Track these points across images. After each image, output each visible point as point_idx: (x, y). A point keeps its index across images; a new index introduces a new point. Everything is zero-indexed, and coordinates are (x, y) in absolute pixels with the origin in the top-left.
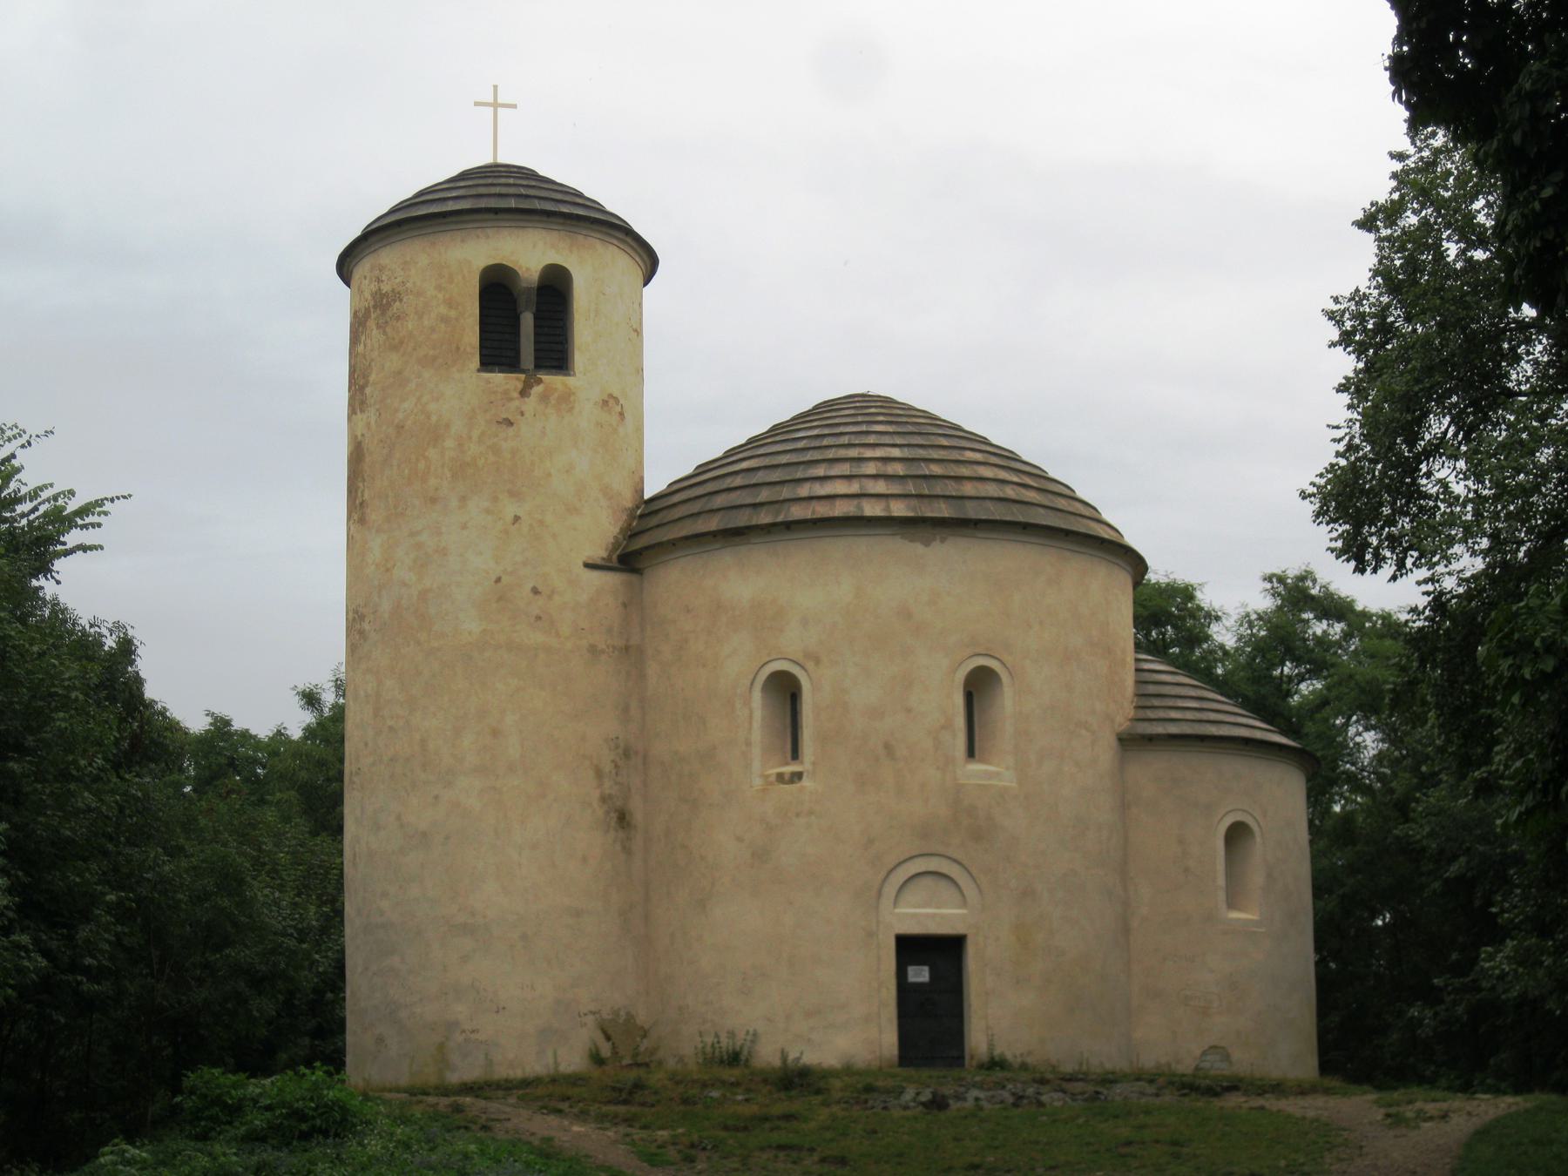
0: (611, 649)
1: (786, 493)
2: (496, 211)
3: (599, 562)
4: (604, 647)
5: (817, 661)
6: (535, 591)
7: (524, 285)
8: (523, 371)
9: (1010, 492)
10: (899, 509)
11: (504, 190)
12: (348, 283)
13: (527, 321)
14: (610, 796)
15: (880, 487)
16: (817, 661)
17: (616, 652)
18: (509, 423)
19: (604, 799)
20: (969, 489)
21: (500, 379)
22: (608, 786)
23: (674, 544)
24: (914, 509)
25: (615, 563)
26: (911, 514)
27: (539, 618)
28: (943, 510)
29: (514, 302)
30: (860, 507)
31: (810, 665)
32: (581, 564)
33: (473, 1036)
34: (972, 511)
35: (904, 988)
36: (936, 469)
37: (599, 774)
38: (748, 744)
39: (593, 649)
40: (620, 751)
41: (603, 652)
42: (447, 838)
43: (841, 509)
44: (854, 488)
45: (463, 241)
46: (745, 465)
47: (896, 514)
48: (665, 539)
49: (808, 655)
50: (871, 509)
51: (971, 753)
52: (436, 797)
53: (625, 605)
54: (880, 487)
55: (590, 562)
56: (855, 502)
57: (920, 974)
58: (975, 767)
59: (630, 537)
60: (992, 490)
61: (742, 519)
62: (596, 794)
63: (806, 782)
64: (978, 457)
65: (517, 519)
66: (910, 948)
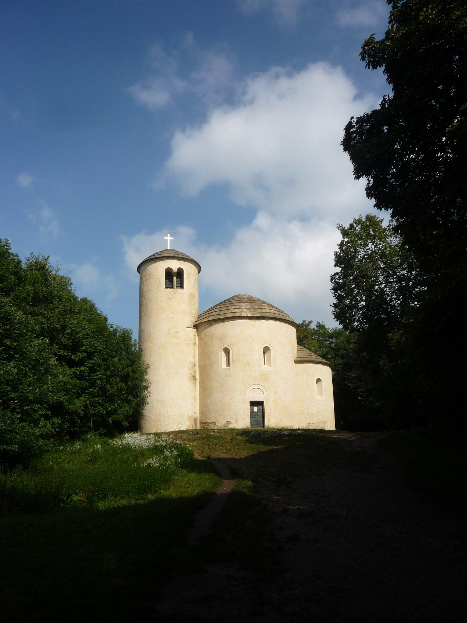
1: (226, 312)
2: (168, 257)
3: (189, 326)
6: (176, 332)
7: (174, 272)
8: (174, 289)
9: (272, 311)
10: (249, 315)
11: (170, 253)
12: (139, 273)
13: (175, 279)
14: (191, 374)
15: (246, 310)
16: (233, 345)
18: (171, 299)
19: (190, 374)
20: (264, 311)
21: (169, 290)
22: (191, 372)
23: (204, 322)
24: (252, 315)
25: (192, 327)
26: (252, 316)
27: (177, 338)
28: (258, 315)
29: (172, 275)
30: (241, 314)
32: (185, 327)
33: (163, 423)
34: (264, 315)
35: (252, 412)
36: (257, 307)
37: (189, 370)
38: (219, 362)
39: (188, 344)
40: (194, 364)
42: (158, 382)
43: (238, 315)
44: (240, 310)
46: (218, 307)
47: (248, 316)
48: (202, 322)
49: (231, 344)
50: (244, 314)
51: (264, 364)
52: (156, 374)
53: (194, 335)
54: (246, 310)
55: (187, 326)
56: (240, 313)
57: (255, 409)
58: (265, 366)
59: (196, 322)
60: (268, 311)
61: (218, 317)
62: (188, 373)
63: (230, 370)
64: (265, 305)
65: (173, 318)
66: (253, 404)
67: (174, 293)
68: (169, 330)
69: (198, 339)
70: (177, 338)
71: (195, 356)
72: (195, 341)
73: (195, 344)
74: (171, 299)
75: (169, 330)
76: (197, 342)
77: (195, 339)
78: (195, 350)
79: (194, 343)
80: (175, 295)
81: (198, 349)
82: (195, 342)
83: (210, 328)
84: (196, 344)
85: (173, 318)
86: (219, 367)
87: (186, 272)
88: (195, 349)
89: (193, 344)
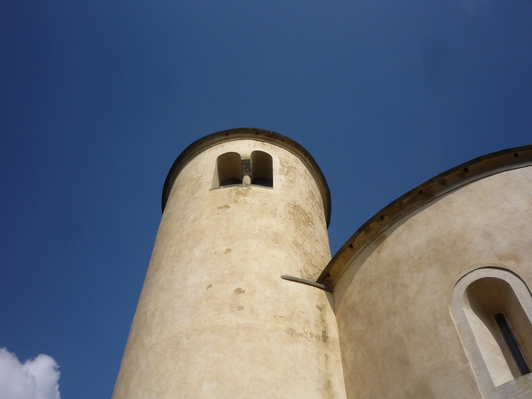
0: (309, 335)
4: (302, 332)
5: (517, 259)
6: (239, 291)
7: (242, 159)
17: (314, 338)
18: (227, 207)
27: (241, 308)
31: (509, 265)
32: (279, 276)
39: (291, 332)
41: (301, 335)
45: (209, 151)
49: (502, 258)
53: (320, 309)
65: (229, 250)
67: (239, 193)
68: (211, 286)
69: (338, 321)
70: (241, 308)
71: (328, 385)
72: (326, 328)
73: (325, 338)
74: (229, 207)
75: (211, 286)
76: (334, 332)
77: (323, 321)
78: (326, 363)
79: (321, 333)
80: (242, 198)
81: (344, 360)
82: (324, 332)
83: (379, 252)
84: (330, 339)
85: (229, 250)
86: (473, 384)
87: (281, 162)
88: (327, 357)
89: (318, 337)
